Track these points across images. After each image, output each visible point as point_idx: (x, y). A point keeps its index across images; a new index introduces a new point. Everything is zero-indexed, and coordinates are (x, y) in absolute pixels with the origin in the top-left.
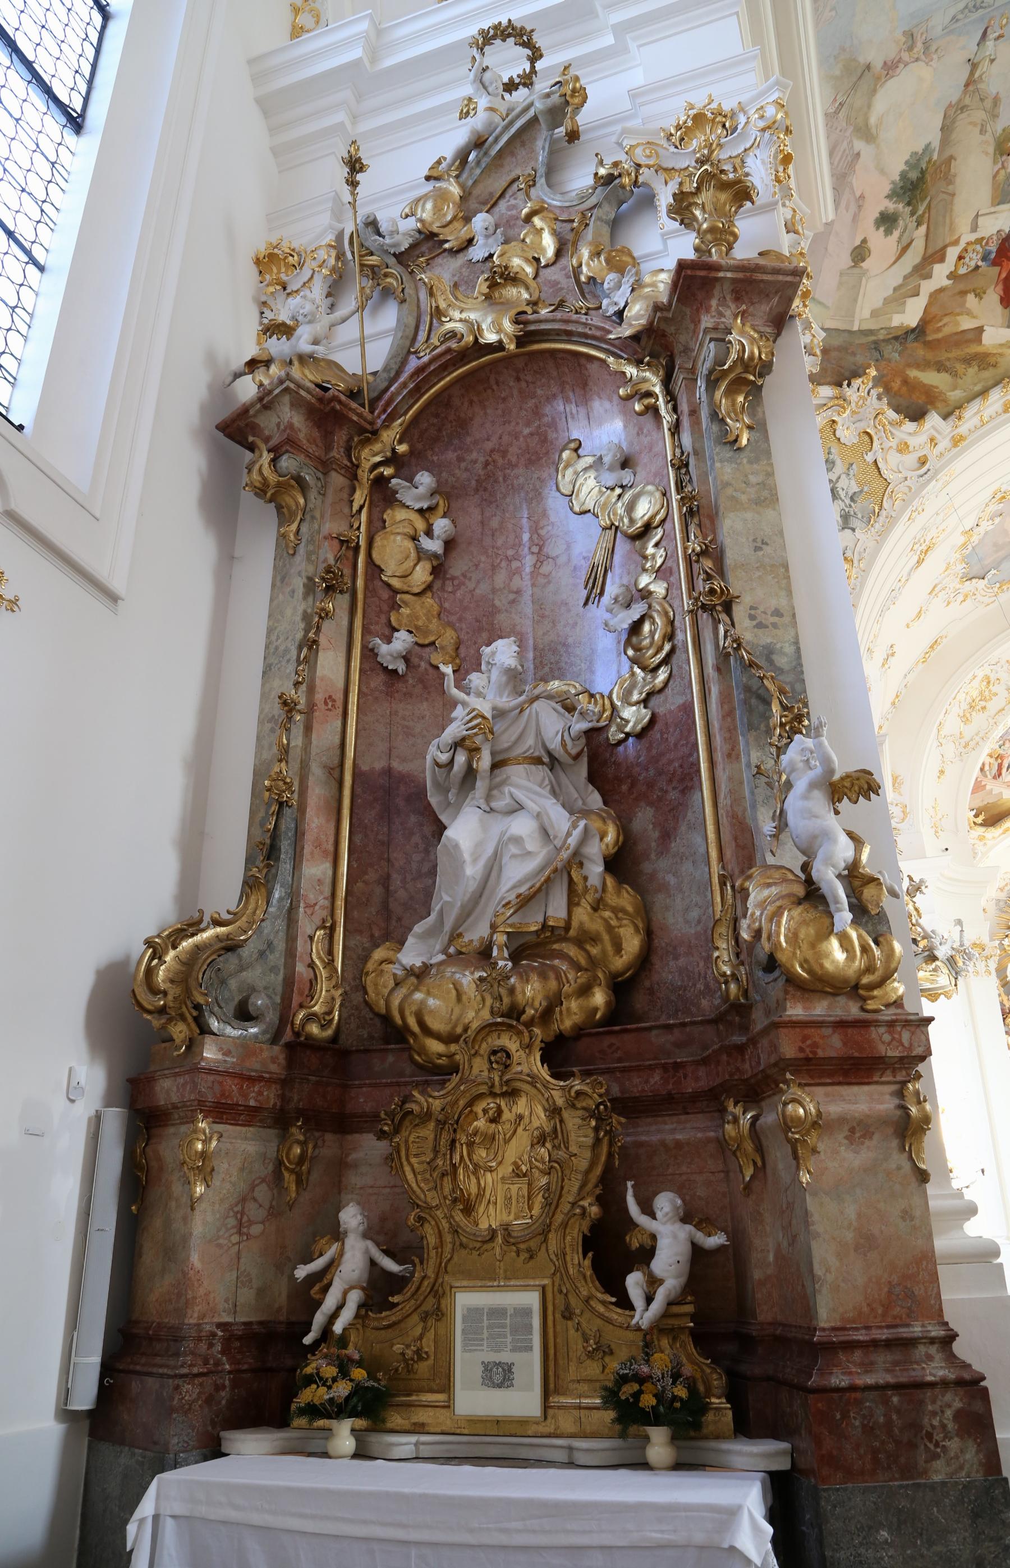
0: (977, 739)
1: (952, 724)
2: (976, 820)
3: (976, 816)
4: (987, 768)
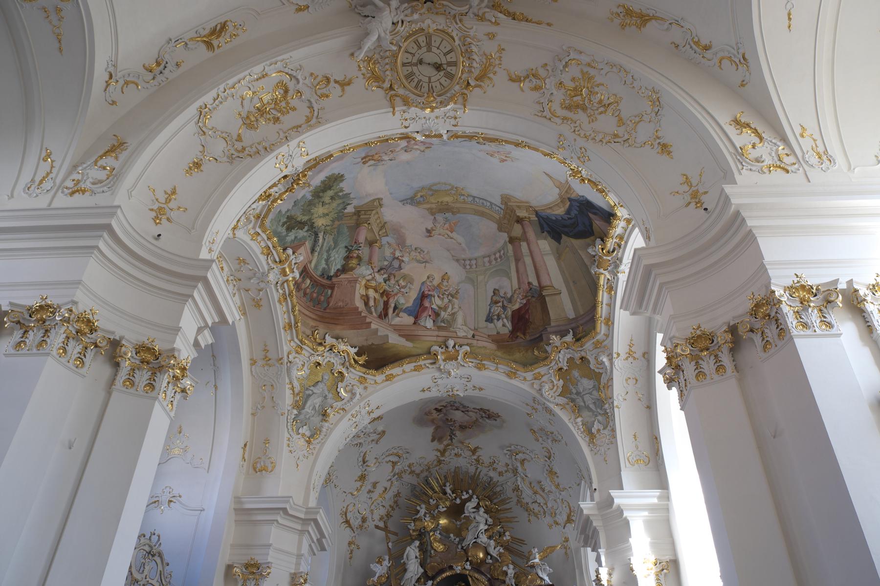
3: (358, 354)
4: (372, 303)
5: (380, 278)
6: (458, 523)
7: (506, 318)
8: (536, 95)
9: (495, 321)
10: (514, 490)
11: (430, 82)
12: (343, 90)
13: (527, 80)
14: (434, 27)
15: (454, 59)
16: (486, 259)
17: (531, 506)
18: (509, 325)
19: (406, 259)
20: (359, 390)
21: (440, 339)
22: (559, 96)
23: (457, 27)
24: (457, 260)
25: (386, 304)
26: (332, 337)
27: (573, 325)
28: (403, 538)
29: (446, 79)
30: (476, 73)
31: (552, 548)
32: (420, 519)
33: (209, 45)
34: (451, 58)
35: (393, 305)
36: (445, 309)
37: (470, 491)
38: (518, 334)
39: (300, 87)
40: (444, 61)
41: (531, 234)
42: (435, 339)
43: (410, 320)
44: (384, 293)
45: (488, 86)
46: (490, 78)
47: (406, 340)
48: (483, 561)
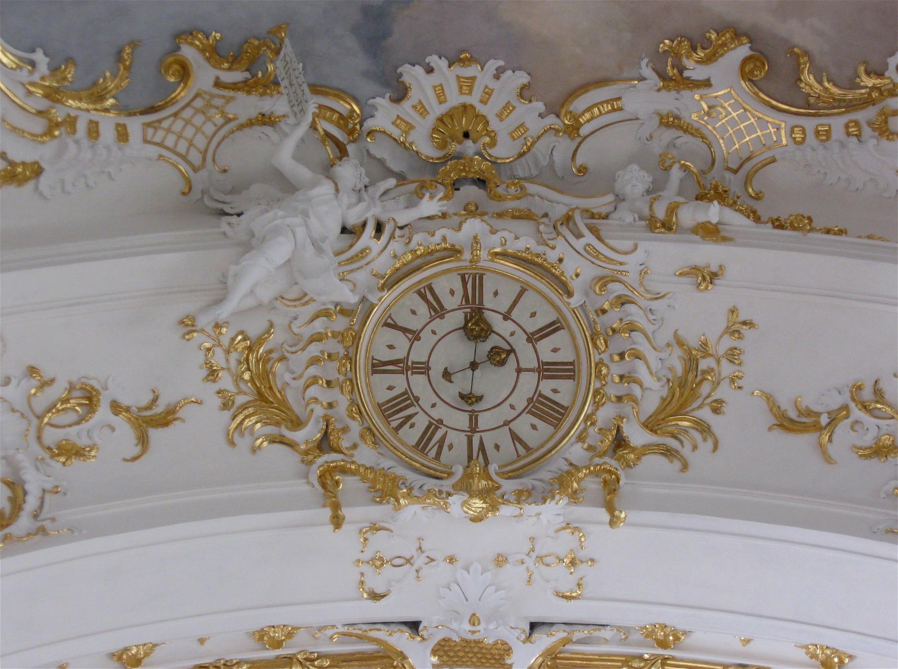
12: (143, 441)
13: (842, 428)
15: (567, 355)
23: (579, 244)
29: (536, 421)
30: (650, 404)
34: (555, 350)
45: (695, 448)
46: (704, 429)
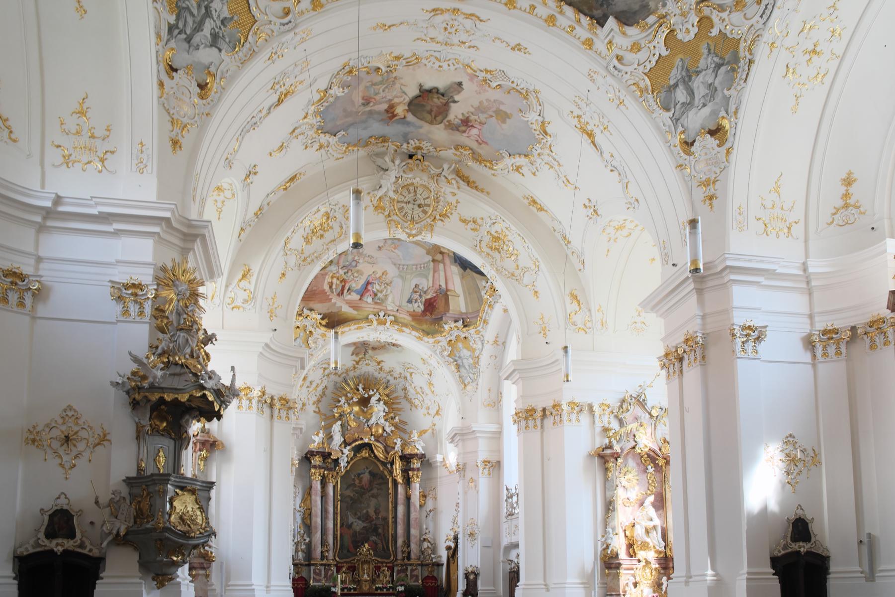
0: (313, 257)
1: (297, 242)
2: (321, 322)
3: (322, 319)
4: (334, 286)
5: (342, 272)
6: (365, 409)
7: (421, 302)
8: (474, 233)
9: (413, 303)
10: (402, 390)
11: (412, 214)
13: (470, 223)
14: (420, 182)
15: (429, 203)
16: (415, 267)
17: (414, 401)
18: (422, 307)
19: (361, 261)
20: (321, 341)
21: (375, 310)
22: (487, 239)
24: (395, 265)
25: (343, 288)
26: (308, 310)
27: (463, 316)
28: (330, 420)
31: (425, 432)
32: (341, 406)
33: (285, 189)
35: (347, 288)
36: (381, 292)
37: (375, 390)
38: (427, 313)
39: (336, 214)
40: (423, 203)
41: (447, 261)
42: (372, 310)
43: (359, 297)
44: (344, 281)
46: (448, 217)
47: (354, 310)
48: (382, 435)
